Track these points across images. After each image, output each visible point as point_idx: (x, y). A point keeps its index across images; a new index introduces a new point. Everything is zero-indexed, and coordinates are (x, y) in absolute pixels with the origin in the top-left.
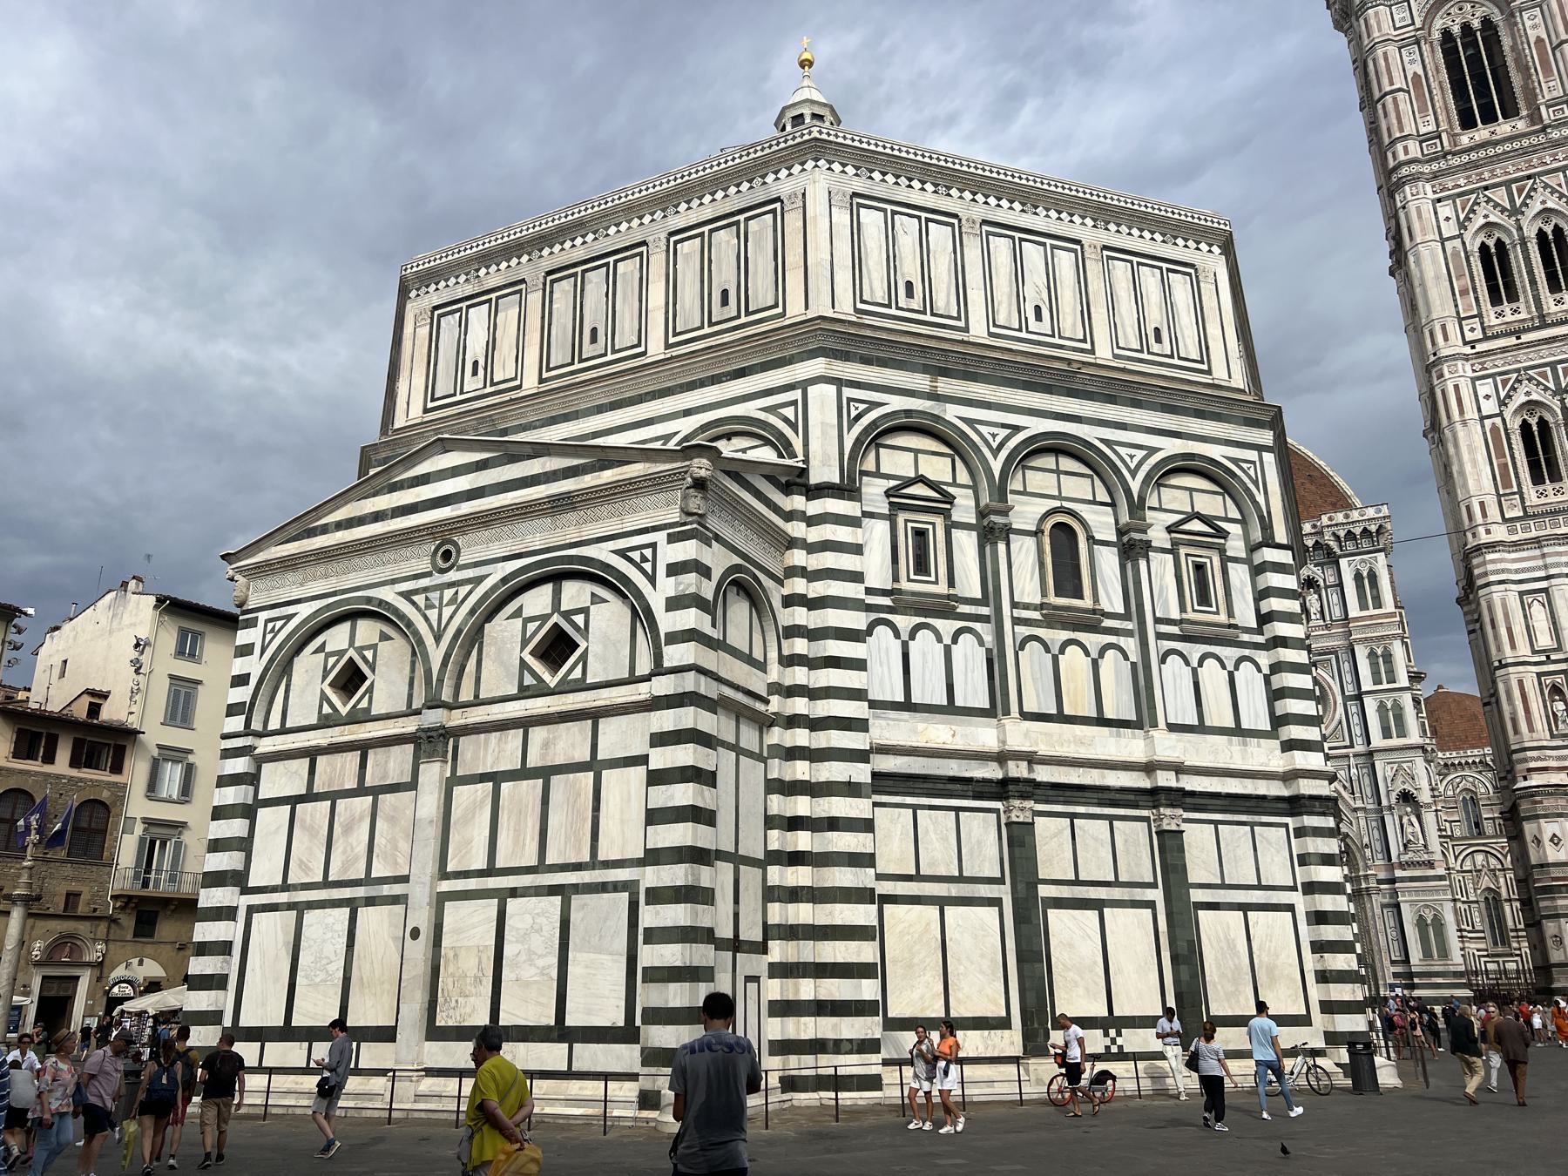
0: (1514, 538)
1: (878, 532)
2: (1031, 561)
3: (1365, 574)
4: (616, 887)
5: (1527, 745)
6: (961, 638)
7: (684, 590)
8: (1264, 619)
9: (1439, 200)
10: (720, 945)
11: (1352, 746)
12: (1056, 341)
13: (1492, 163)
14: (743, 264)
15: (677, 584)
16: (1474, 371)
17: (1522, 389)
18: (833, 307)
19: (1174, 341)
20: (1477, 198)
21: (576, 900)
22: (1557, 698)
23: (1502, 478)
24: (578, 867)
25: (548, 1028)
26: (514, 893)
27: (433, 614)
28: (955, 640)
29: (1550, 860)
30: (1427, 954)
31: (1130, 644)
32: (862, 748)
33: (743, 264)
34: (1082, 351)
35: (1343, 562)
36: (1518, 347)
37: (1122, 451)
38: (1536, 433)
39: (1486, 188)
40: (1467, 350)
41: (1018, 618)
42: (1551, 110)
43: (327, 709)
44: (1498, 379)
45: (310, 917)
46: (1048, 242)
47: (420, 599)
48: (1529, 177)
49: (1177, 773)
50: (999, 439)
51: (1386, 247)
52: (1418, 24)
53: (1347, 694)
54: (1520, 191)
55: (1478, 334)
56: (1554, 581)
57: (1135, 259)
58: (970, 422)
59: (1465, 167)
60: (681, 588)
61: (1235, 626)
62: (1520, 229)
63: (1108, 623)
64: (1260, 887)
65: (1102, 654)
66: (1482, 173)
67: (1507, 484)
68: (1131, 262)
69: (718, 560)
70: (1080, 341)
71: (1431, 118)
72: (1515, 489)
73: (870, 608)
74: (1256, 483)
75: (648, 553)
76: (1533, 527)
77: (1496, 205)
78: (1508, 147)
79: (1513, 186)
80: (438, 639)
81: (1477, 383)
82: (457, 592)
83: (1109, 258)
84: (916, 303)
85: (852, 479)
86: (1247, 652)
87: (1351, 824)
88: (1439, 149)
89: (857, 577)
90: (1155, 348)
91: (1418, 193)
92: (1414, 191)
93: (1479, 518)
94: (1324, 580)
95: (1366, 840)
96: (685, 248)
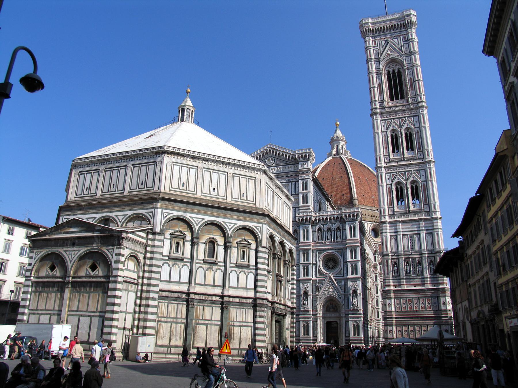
0: (391, 220)
1: (167, 243)
2: (202, 250)
5: (386, 278)
6: (184, 267)
8: (257, 263)
9: (382, 120)
10: (119, 329)
11: (344, 276)
12: (218, 197)
13: (396, 112)
15: (117, 258)
16: (386, 171)
17: (397, 178)
19: (247, 196)
20: (391, 121)
24: (94, 312)
25: (86, 342)
26: (82, 316)
27: (70, 256)
28: (182, 267)
29: (388, 310)
30: (355, 335)
31: (223, 268)
34: (224, 199)
35: (347, 223)
37: (228, 224)
39: (394, 119)
41: (198, 262)
43: (47, 273)
44: (392, 174)
45: (42, 316)
46: (219, 172)
50: (198, 222)
58: (192, 218)
61: (250, 265)
64: (245, 322)
65: (216, 271)
68: (240, 177)
69: (126, 252)
70: (223, 197)
73: (163, 260)
74: (260, 232)
75: (112, 250)
77: (396, 124)
80: (71, 262)
83: (234, 176)
84: (185, 188)
85: (163, 231)
86: (252, 271)
89: (161, 253)
94: (342, 228)
95: (343, 303)
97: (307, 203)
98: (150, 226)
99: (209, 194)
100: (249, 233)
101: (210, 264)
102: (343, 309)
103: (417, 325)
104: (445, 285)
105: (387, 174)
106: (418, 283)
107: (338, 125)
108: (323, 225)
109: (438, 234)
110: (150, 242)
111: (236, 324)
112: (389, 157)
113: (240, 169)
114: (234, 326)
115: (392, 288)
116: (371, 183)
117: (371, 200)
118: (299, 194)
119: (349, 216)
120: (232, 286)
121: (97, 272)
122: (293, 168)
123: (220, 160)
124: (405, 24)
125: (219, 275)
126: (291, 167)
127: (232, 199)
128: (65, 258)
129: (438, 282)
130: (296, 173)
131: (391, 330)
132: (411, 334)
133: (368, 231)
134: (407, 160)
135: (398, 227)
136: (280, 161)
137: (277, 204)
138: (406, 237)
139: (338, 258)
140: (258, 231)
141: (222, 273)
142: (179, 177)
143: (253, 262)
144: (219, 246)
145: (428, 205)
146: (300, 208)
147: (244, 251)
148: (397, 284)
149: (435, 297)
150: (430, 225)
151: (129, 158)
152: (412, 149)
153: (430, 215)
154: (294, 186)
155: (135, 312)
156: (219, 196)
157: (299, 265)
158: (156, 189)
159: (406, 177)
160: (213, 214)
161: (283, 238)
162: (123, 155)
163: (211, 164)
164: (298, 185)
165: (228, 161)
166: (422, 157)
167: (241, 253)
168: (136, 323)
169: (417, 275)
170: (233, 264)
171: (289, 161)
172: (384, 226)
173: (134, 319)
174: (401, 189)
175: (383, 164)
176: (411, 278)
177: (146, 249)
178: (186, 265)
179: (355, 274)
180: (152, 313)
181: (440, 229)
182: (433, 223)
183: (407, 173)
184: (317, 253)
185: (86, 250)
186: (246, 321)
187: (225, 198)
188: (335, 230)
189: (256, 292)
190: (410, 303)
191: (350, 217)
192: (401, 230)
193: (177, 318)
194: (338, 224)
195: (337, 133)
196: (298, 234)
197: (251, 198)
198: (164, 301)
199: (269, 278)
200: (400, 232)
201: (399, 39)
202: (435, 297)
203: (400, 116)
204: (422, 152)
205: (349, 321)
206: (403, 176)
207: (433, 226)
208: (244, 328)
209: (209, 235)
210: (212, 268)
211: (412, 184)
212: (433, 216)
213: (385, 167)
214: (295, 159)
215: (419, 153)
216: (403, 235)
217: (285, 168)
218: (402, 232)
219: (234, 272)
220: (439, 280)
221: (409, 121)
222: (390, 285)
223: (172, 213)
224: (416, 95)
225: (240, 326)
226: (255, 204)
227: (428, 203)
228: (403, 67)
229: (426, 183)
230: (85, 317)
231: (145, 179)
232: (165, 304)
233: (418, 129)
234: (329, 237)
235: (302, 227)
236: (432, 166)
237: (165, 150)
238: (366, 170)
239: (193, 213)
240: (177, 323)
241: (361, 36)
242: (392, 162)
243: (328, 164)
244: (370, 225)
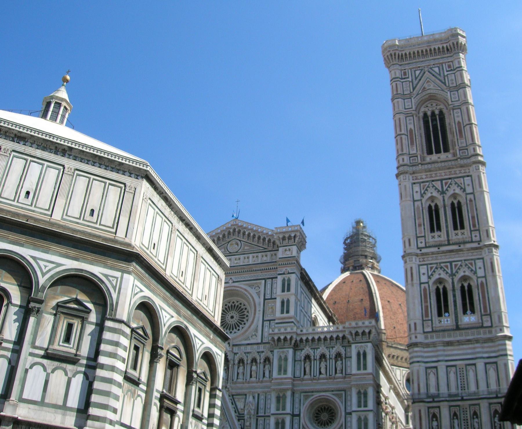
0: (426, 341)
3: (362, 353)
9: (414, 183)
12: (33, 208)
16: (420, 261)
19: (100, 216)
20: (429, 184)
22: (434, 419)
23: (425, 313)
34: (45, 214)
35: (353, 346)
36: (438, 253)
37: (42, 263)
38: (441, 293)
39: (433, 181)
40: (418, 251)
42: (461, 151)
44: (429, 266)
46: (46, 163)
48: (450, 179)
52: (414, 108)
54: (446, 184)
55: (423, 245)
56: (440, 363)
57: (92, 177)
59: (426, 171)
61: (80, 356)
62: (444, 200)
66: (432, 174)
67: (427, 316)
68: (89, 178)
70: (46, 210)
71: (415, 148)
72: (430, 318)
74: (115, 288)
76: (435, 337)
77: (436, 189)
78: (443, 164)
81: (421, 267)
88: (417, 161)
91: (406, 179)
92: (404, 178)
94: (345, 354)
97: (288, 312)
99: (14, 201)
108: (314, 349)
112: (425, 240)
118: (275, 298)
120: (30, 398)
122: (269, 257)
124: (449, 48)
126: (266, 256)
130: (274, 265)
133: (401, 382)
134: (453, 244)
136: (249, 246)
137: (181, 254)
138: (453, 369)
145: (489, 316)
146: (277, 321)
147: (70, 326)
152: (462, 227)
153: (493, 332)
154: (269, 286)
156: (35, 206)
157: (269, 416)
161: (185, 323)
164: (275, 284)
166: (478, 239)
170: (41, 348)
171: (264, 246)
184: (302, 397)
188: (333, 357)
194: (338, 348)
196: (270, 366)
197: (108, 219)
199: (134, 395)
201: (441, 68)
203: (442, 176)
204: (478, 232)
206: (448, 269)
214: (274, 243)
215: (473, 232)
216: (447, 366)
217: (257, 257)
224: (467, 146)
226: (116, 233)
228: (447, 105)
229: (486, 280)
233: (471, 196)
234: (323, 371)
235: (278, 352)
241: (384, 65)
242: (430, 247)
243: (344, 282)
244: (404, 372)
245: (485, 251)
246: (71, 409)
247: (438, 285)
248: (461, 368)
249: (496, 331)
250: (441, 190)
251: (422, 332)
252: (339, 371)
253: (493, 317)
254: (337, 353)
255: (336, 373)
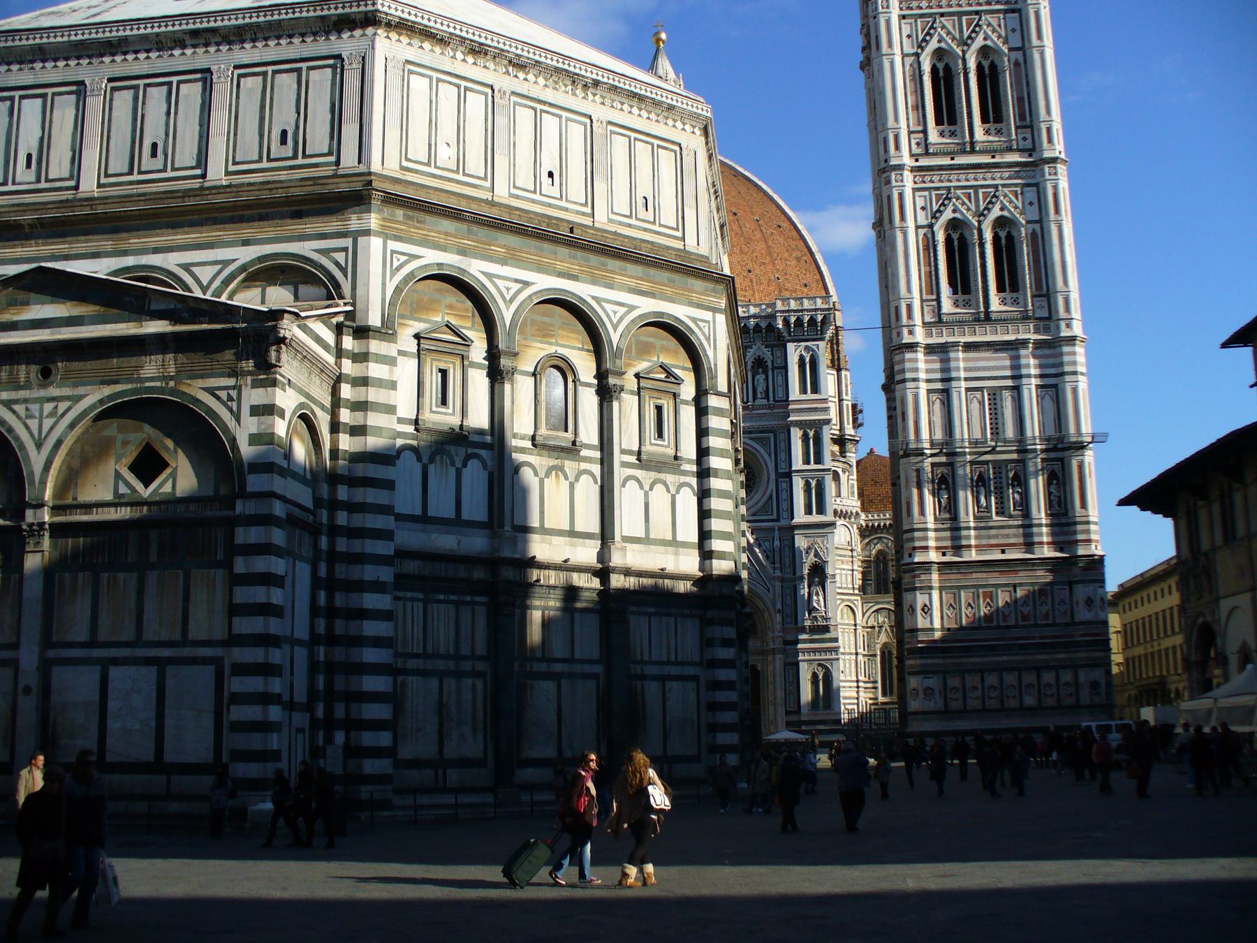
0: (930, 341)
1: (406, 371)
3: (808, 360)
4: (205, 661)
5: (916, 526)
6: (470, 463)
7: (265, 429)
9: (904, 17)
11: (778, 520)
12: (563, 204)
14: (301, 107)
15: (259, 424)
16: (915, 183)
17: (950, 208)
18: (383, 165)
21: (170, 670)
22: (944, 486)
26: (115, 662)
27: (33, 424)
28: (465, 465)
29: (920, 625)
32: (386, 553)
33: (301, 107)
34: (584, 214)
35: (791, 347)
38: (956, 248)
39: (942, 15)
44: (934, 193)
46: (564, 114)
47: (19, 408)
49: (625, 575)
50: (512, 292)
51: (859, 41)
53: (780, 471)
57: (633, 135)
58: (489, 276)
60: (263, 427)
63: (584, 453)
64: (677, 663)
65: (577, 479)
70: (582, 205)
74: (708, 339)
75: (234, 393)
77: (949, 33)
79: (964, 18)
80: (39, 446)
82: (56, 407)
83: (612, 132)
87: (769, 591)
89: (391, 409)
90: (642, 214)
93: (904, 320)
94: (773, 361)
95: (779, 606)
96: (248, 83)
98: (341, 302)
99: (535, 192)
100: (673, 343)
101: (556, 454)
102: (779, 627)
103: (1010, 669)
104: (1093, 547)
105: (917, 194)
106: (1013, 541)
107: (663, 42)
109: (1075, 390)
110: (348, 367)
111: (650, 670)
112: (926, 139)
113: (631, 107)
114: (643, 677)
115: (933, 556)
116: (772, 234)
117: (772, 288)
119: (799, 322)
121: (169, 484)
123: (566, 67)
125: (588, 492)
127: (612, 216)
128: (10, 430)
129: (1073, 538)
131: (929, 688)
132: (990, 698)
134: (982, 152)
135: (953, 364)
138: (978, 394)
139: (758, 460)
140: (701, 337)
141: (597, 489)
142: (431, 121)
143: (689, 449)
144: (580, 387)
147: (659, 409)
148: (948, 543)
149: (1063, 583)
150: (1051, 361)
151: (219, 39)
153: (1052, 329)
155: (315, 639)
158: (349, 159)
159: (977, 206)
160: (561, 266)
162: (191, 26)
163: (536, 82)
165: (594, 76)
166: (1028, 144)
167: (650, 415)
168: (321, 681)
169: (1011, 516)
170: (629, 452)
172: (911, 360)
173: (313, 667)
174: (963, 241)
175: (907, 161)
176: (991, 524)
177: (335, 392)
178: (477, 456)
179: (817, 513)
180: (377, 642)
181: (1082, 374)
182: (1061, 354)
183: (983, 193)
185: (111, 398)
186: (679, 660)
187: (588, 210)
189: (706, 555)
190: (988, 604)
191: (802, 325)
192: (962, 374)
193: (458, 657)
195: (660, 66)
198: (409, 595)
200: (958, 379)
202: (1063, 583)
204: (1029, 130)
205: (797, 664)
206: (970, 201)
207: (1061, 364)
208: (675, 684)
209: (545, 346)
210: (560, 469)
211: (998, 230)
212: (1062, 335)
213: (913, 170)
215: (1019, 130)
216: (967, 390)
218: (966, 379)
219: (632, 484)
220: (1075, 533)
221: (989, 25)
222: (926, 548)
223: (419, 257)
225: (663, 679)
226: (683, 239)
227: (1045, 292)
229: (1042, 229)
230: (133, 668)
231: (293, 123)
232: (415, 604)
233: (1019, 55)
236: (1060, 177)
237: (377, 11)
238: (753, 192)
239: (490, 259)
240: (459, 675)
245: (1043, 170)
246: (684, 545)
247: (950, 232)
248: (992, 393)
249: (1058, 328)
250: (958, 36)
251: (920, 324)
252: (761, 393)
253: (1052, 300)
254: (755, 359)
255: (755, 398)
